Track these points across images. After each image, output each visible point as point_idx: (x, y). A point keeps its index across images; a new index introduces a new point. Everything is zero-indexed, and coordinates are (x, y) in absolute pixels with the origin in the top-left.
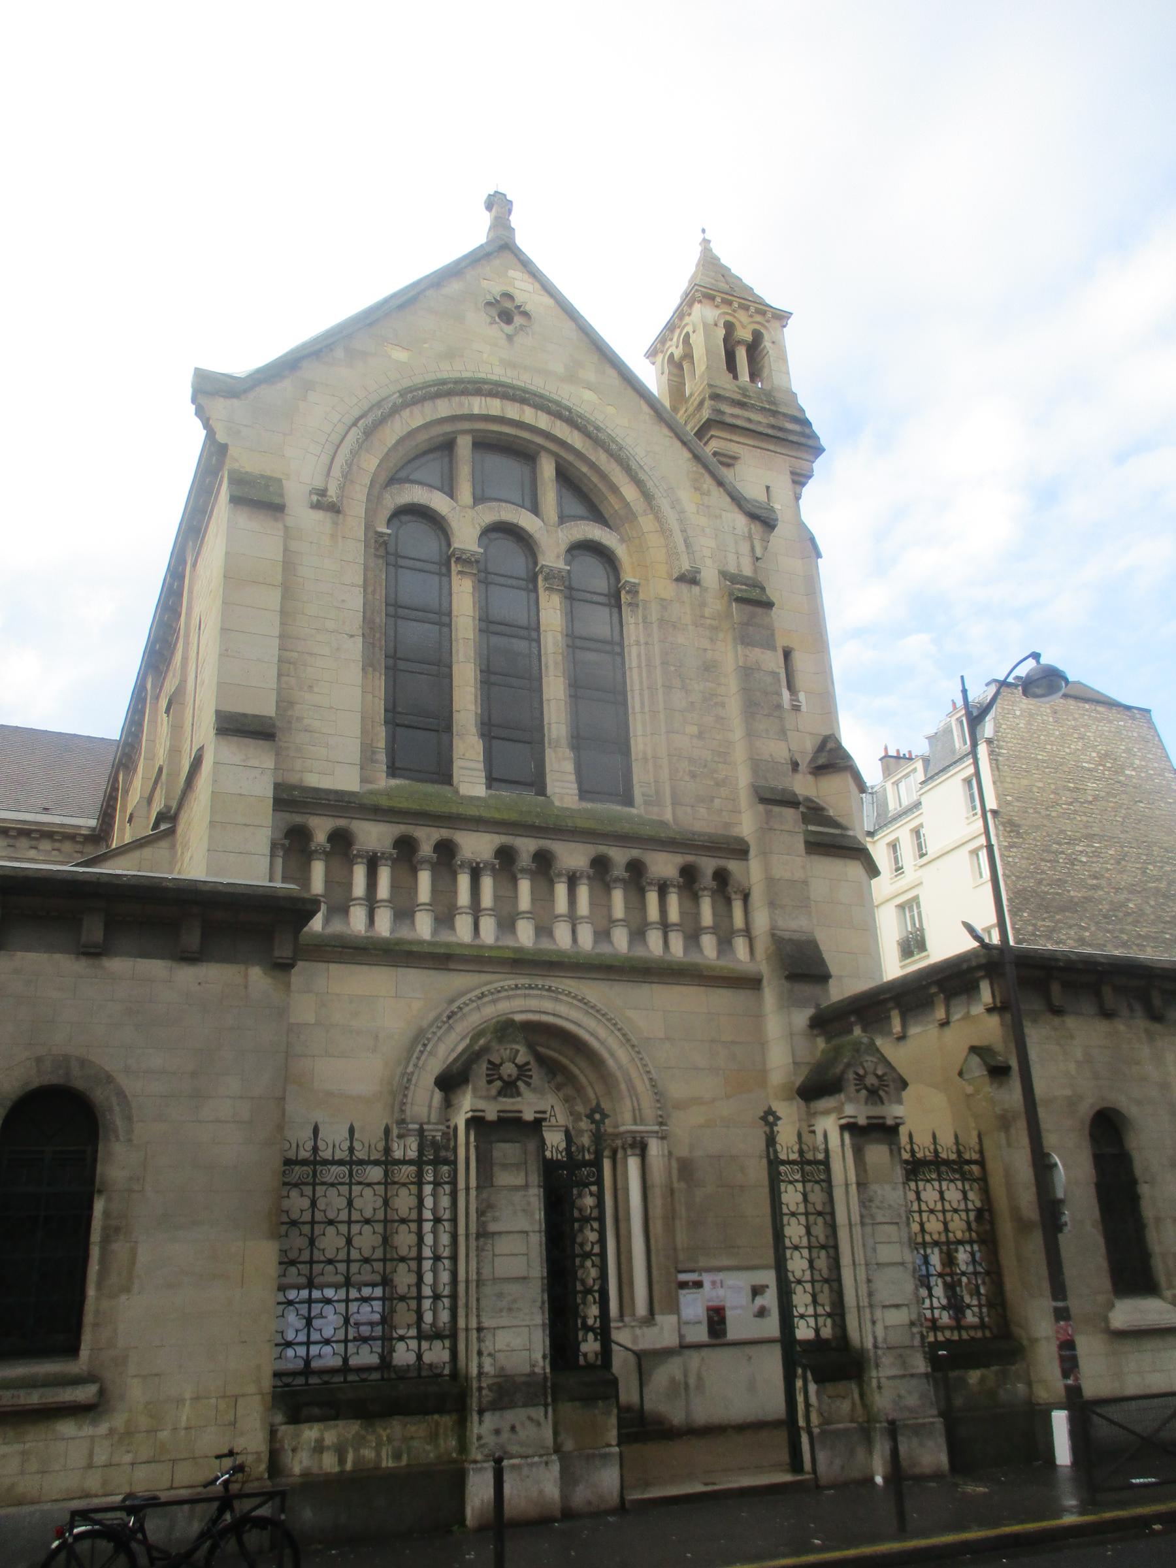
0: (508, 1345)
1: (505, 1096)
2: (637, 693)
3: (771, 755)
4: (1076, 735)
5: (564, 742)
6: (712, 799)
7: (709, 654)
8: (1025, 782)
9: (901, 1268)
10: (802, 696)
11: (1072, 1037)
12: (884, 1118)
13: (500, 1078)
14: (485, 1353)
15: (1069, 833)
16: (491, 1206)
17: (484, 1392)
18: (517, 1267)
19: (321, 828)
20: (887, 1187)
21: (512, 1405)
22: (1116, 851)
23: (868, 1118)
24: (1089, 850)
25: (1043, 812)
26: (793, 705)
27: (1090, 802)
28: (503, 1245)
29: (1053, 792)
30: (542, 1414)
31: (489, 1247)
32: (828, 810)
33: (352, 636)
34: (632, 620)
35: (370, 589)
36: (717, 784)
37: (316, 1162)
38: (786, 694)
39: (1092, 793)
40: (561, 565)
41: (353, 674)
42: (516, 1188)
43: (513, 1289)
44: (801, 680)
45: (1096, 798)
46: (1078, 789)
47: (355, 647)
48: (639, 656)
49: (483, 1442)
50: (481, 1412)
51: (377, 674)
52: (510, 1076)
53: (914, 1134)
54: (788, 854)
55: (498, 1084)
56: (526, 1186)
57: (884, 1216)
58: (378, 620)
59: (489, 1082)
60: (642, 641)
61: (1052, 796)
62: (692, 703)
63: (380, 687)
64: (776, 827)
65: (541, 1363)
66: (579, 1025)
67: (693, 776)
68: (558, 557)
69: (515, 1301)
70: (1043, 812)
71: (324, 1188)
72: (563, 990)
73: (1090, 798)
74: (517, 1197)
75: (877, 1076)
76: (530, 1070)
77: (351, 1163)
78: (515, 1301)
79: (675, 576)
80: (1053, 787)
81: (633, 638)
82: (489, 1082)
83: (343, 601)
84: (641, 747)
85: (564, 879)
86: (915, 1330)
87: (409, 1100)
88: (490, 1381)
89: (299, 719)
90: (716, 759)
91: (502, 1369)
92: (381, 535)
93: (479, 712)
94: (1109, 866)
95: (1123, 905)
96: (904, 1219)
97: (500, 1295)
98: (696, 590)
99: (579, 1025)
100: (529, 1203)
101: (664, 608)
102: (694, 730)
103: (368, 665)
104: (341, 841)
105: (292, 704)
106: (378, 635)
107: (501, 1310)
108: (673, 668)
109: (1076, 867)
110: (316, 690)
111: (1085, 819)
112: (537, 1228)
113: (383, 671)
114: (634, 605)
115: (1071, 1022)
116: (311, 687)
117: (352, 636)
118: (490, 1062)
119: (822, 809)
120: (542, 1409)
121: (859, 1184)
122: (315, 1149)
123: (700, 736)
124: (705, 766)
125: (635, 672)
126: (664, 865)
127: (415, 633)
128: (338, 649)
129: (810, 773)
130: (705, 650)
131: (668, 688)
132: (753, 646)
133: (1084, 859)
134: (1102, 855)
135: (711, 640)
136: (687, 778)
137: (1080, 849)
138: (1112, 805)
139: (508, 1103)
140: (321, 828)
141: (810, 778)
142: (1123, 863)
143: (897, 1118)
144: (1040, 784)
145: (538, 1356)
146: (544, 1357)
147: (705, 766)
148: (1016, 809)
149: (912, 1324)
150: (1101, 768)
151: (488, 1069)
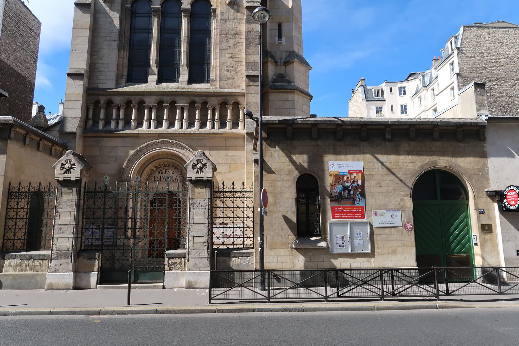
0: (61, 242)
1: (66, 174)
2: (213, 46)
3: (254, 60)
4: (498, 41)
5: (185, 65)
6: (234, 79)
7: (238, 29)
8: (473, 61)
9: (203, 225)
10: (283, 39)
11: (295, 148)
12: (203, 177)
13: (65, 168)
14: (54, 244)
15: (490, 78)
16: (59, 205)
17: (53, 255)
18: (67, 221)
19: (103, 100)
20: (202, 200)
21: (61, 258)
22: (511, 83)
23: (196, 178)
24: (499, 83)
25: (480, 72)
26: (279, 42)
27: (502, 66)
28: (62, 215)
29: (484, 64)
30: (70, 261)
31: (58, 216)
32: (287, 77)
33: (114, 41)
34: (213, 21)
35: (123, 25)
36: (237, 73)
37: (19, 192)
38: (277, 38)
39: (504, 62)
40: (189, 7)
41: (114, 53)
42: (69, 199)
43: (65, 227)
44: (284, 33)
45: (504, 64)
46: (496, 61)
47: (115, 44)
48: (214, 33)
49: (51, 267)
50: (51, 260)
51: (125, 52)
52: (68, 167)
53: (11, 184)
54: (255, 93)
55: (65, 170)
56: (72, 199)
57: (199, 209)
58: (126, 35)
59: (61, 170)
60: (215, 28)
61: (485, 65)
62: (230, 46)
63: (126, 55)
64: (251, 84)
65: (71, 248)
66: (179, 152)
67: (228, 71)
68: (188, 4)
69: (65, 231)
70: (480, 72)
71: (246, 198)
72: (174, 142)
73: (502, 64)
74: (68, 202)
75: (203, 164)
76: (75, 166)
77: (95, 192)
78: (65, 231)
79: (227, 3)
80: (485, 62)
81: (213, 27)
82: (61, 170)
83: (112, 30)
84: (213, 64)
85: (180, 108)
86: (205, 244)
87: (124, 175)
88: (55, 252)
89: (98, 68)
90: (237, 64)
91: (59, 249)
92: (127, 7)
93: (158, 59)
94: (508, 89)
95: (513, 102)
96: (207, 209)
97: (60, 229)
98: (236, 7)
99: (179, 152)
100: (72, 204)
101: (223, 15)
102: (230, 55)
103: (120, 49)
104: (109, 103)
105: (95, 64)
106: (126, 39)
107: (60, 233)
108: (224, 36)
109: (492, 90)
110: (103, 59)
111: (498, 72)
112: (74, 211)
113: (128, 50)
114: (214, 17)
115: (296, 143)
116: (101, 58)
117: (114, 41)
118: (62, 164)
119: (285, 77)
120: (70, 260)
121: (190, 198)
122: (95, 189)
123: (232, 57)
124: (233, 67)
125: (213, 38)
126: (214, 102)
127: (139, 37)
128: (110, 45)
129: (283, 65)
130: (237, 27)
131: (221, 42)
132: (251, 23)
133: (496, 87)
134: (505, 85)
135: (239, 23)
136: (225, 72)
137: (495, 83)
138: (512, 66)
139: (67, 175)
140: (103, 100)
141: (283, 67)
142: (514, 87)
143: (208, 178)
144: (480, 62)
145: (71, 246)
146: (72, 246)
147: (233, 67)
148: (467, 72)
149: (204, 242)
150: (509, 52)
151: (61, 166)
